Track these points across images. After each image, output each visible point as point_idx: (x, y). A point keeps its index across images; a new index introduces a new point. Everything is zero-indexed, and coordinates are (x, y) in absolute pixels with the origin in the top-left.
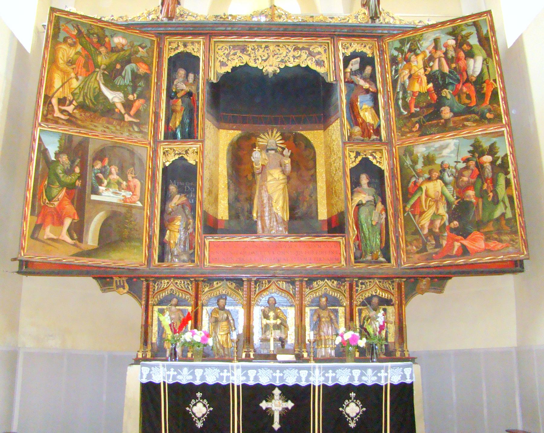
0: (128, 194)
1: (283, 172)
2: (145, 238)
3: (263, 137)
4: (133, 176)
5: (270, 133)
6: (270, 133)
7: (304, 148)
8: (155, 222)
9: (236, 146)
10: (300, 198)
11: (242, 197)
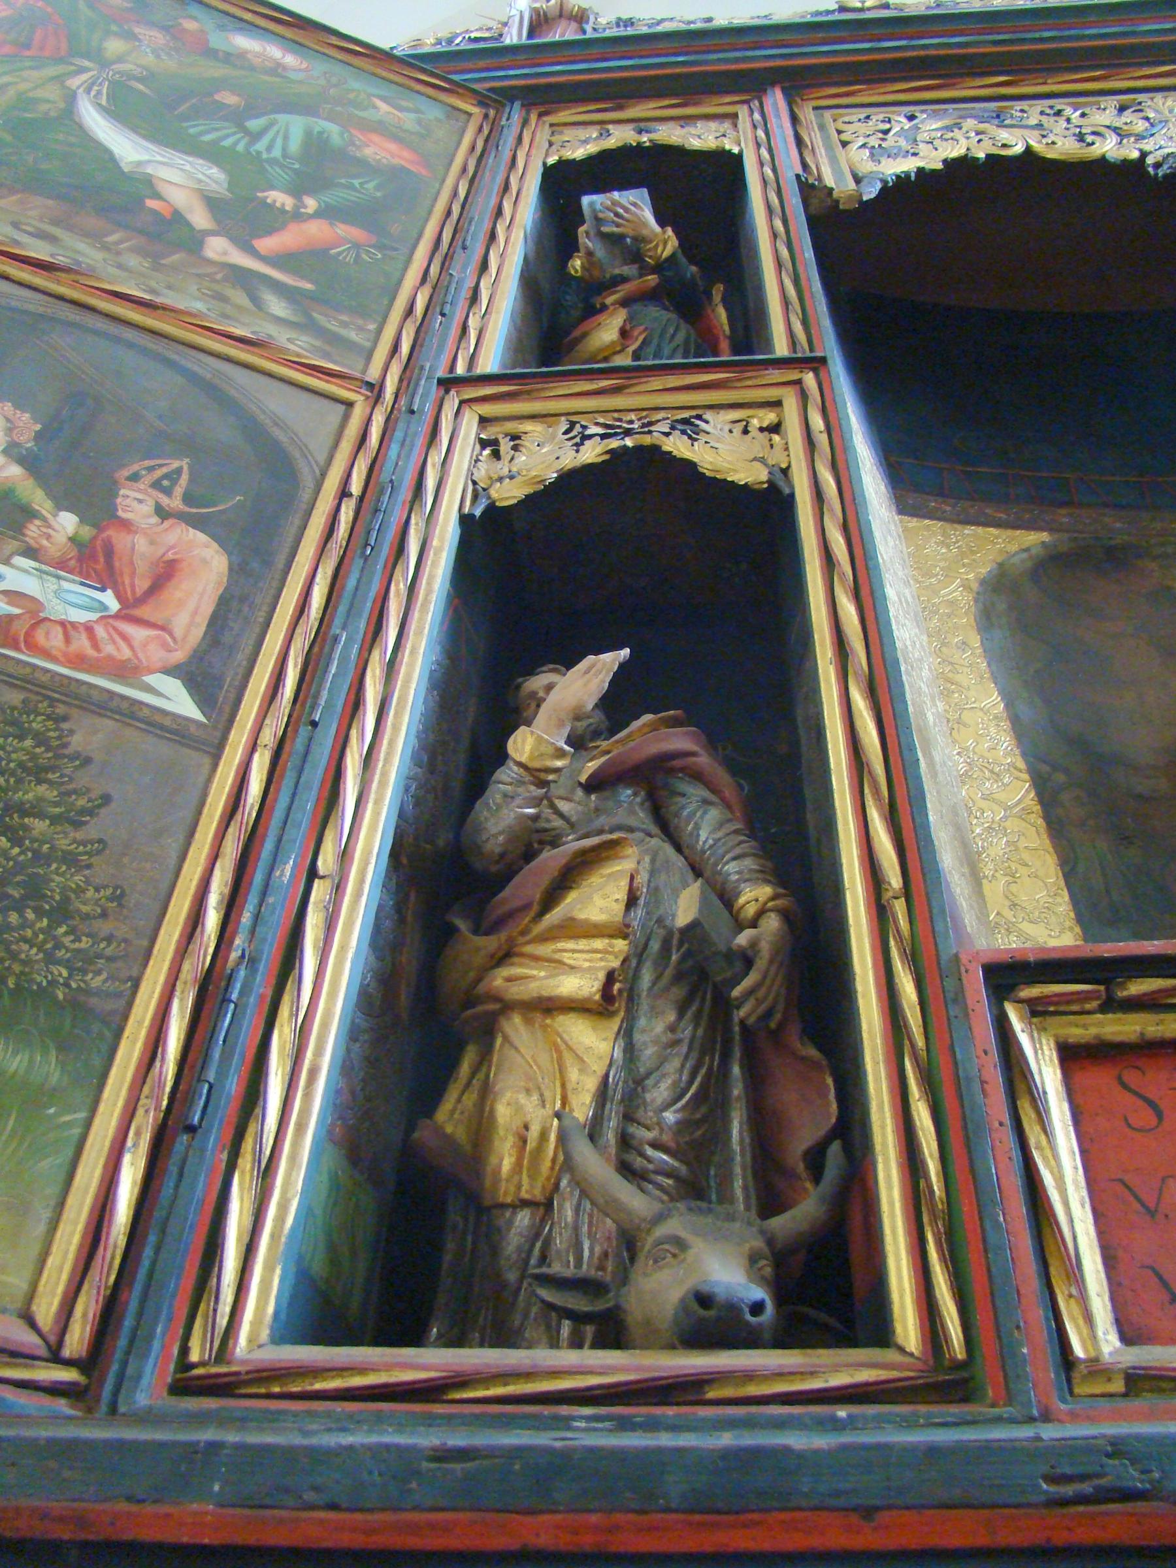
0: (73, 601)
2: (156, 1010)
4: (175, 502)
8: (326, 862)
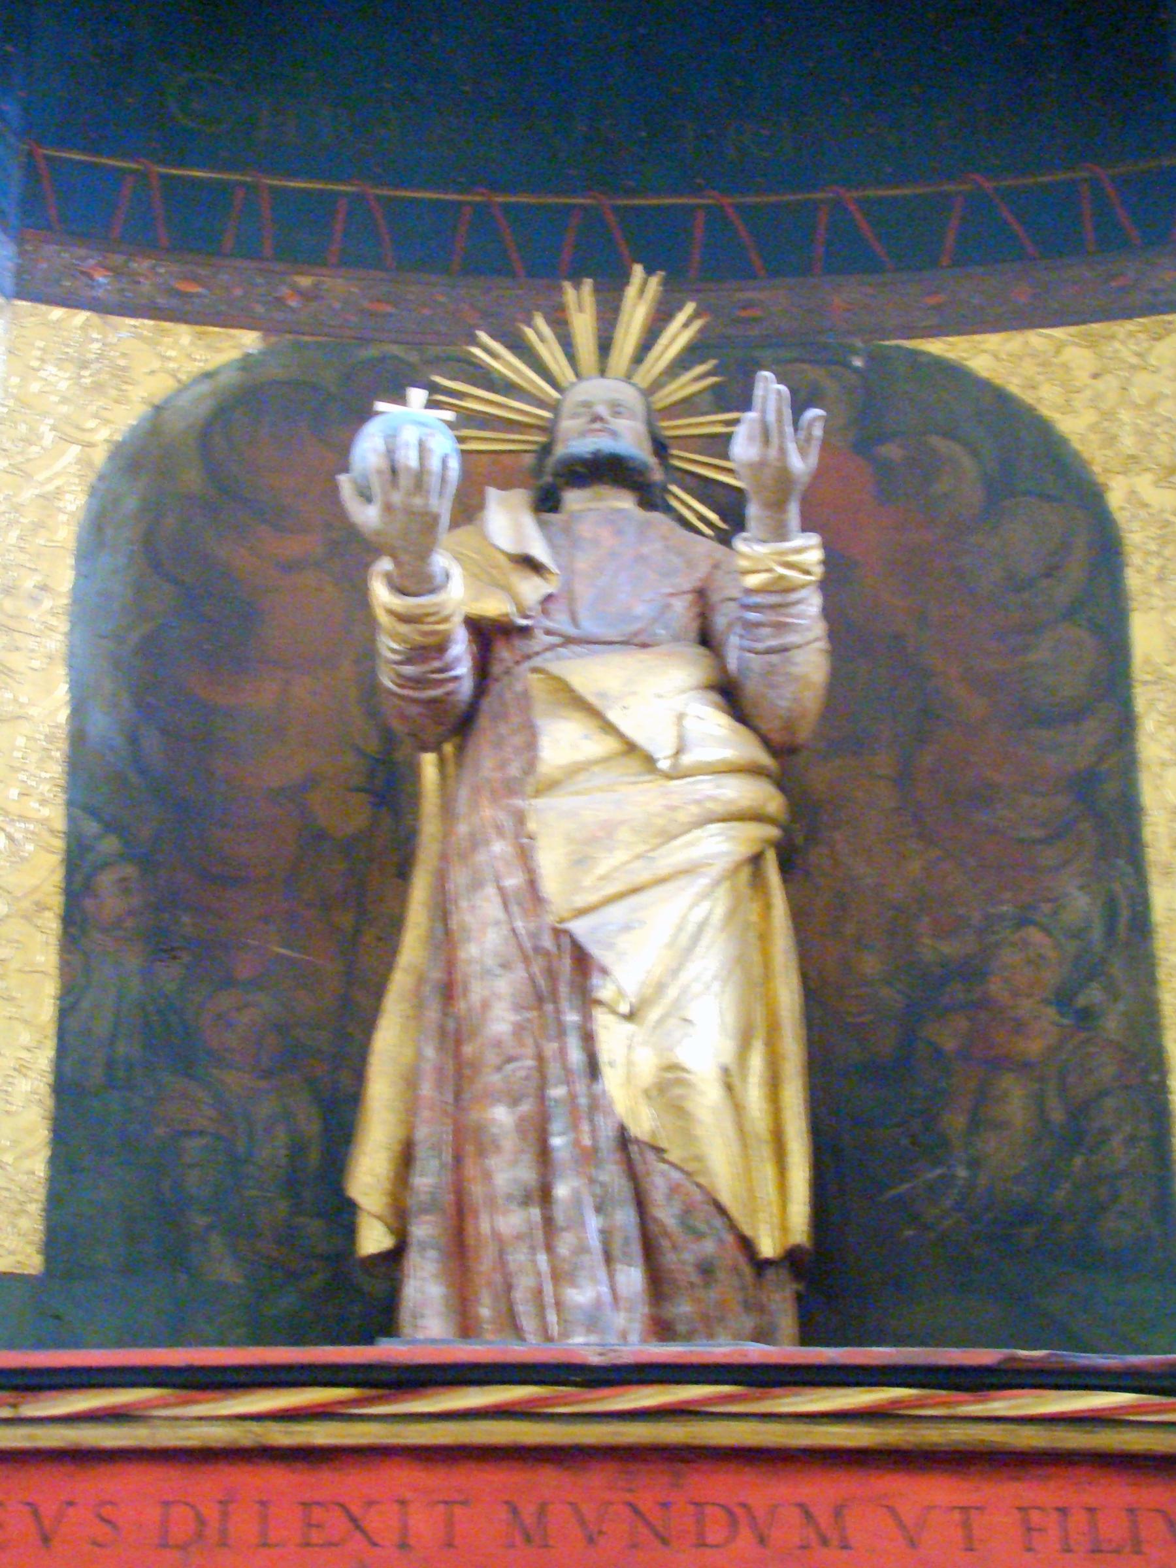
1: (730, 694)
3: (507, 364)
5: (583, 325)
6: (583, 325)
7: (972, 494)
9: (192, 478)
10: (948, 1036)
11: (239, 1018)
